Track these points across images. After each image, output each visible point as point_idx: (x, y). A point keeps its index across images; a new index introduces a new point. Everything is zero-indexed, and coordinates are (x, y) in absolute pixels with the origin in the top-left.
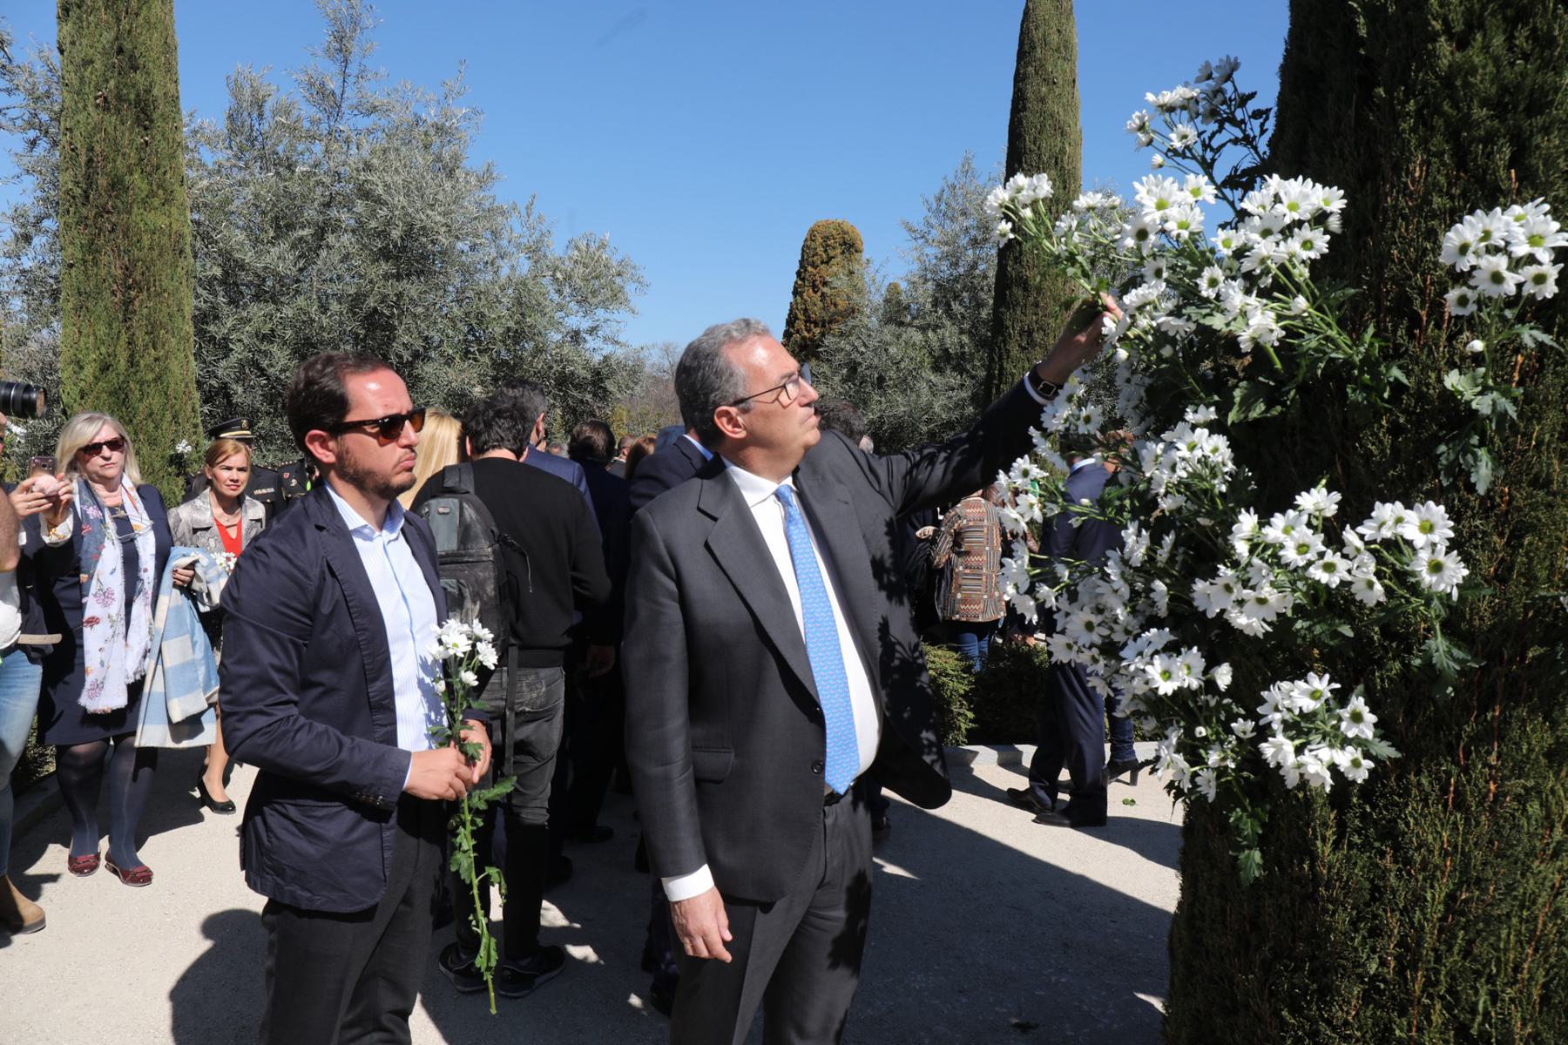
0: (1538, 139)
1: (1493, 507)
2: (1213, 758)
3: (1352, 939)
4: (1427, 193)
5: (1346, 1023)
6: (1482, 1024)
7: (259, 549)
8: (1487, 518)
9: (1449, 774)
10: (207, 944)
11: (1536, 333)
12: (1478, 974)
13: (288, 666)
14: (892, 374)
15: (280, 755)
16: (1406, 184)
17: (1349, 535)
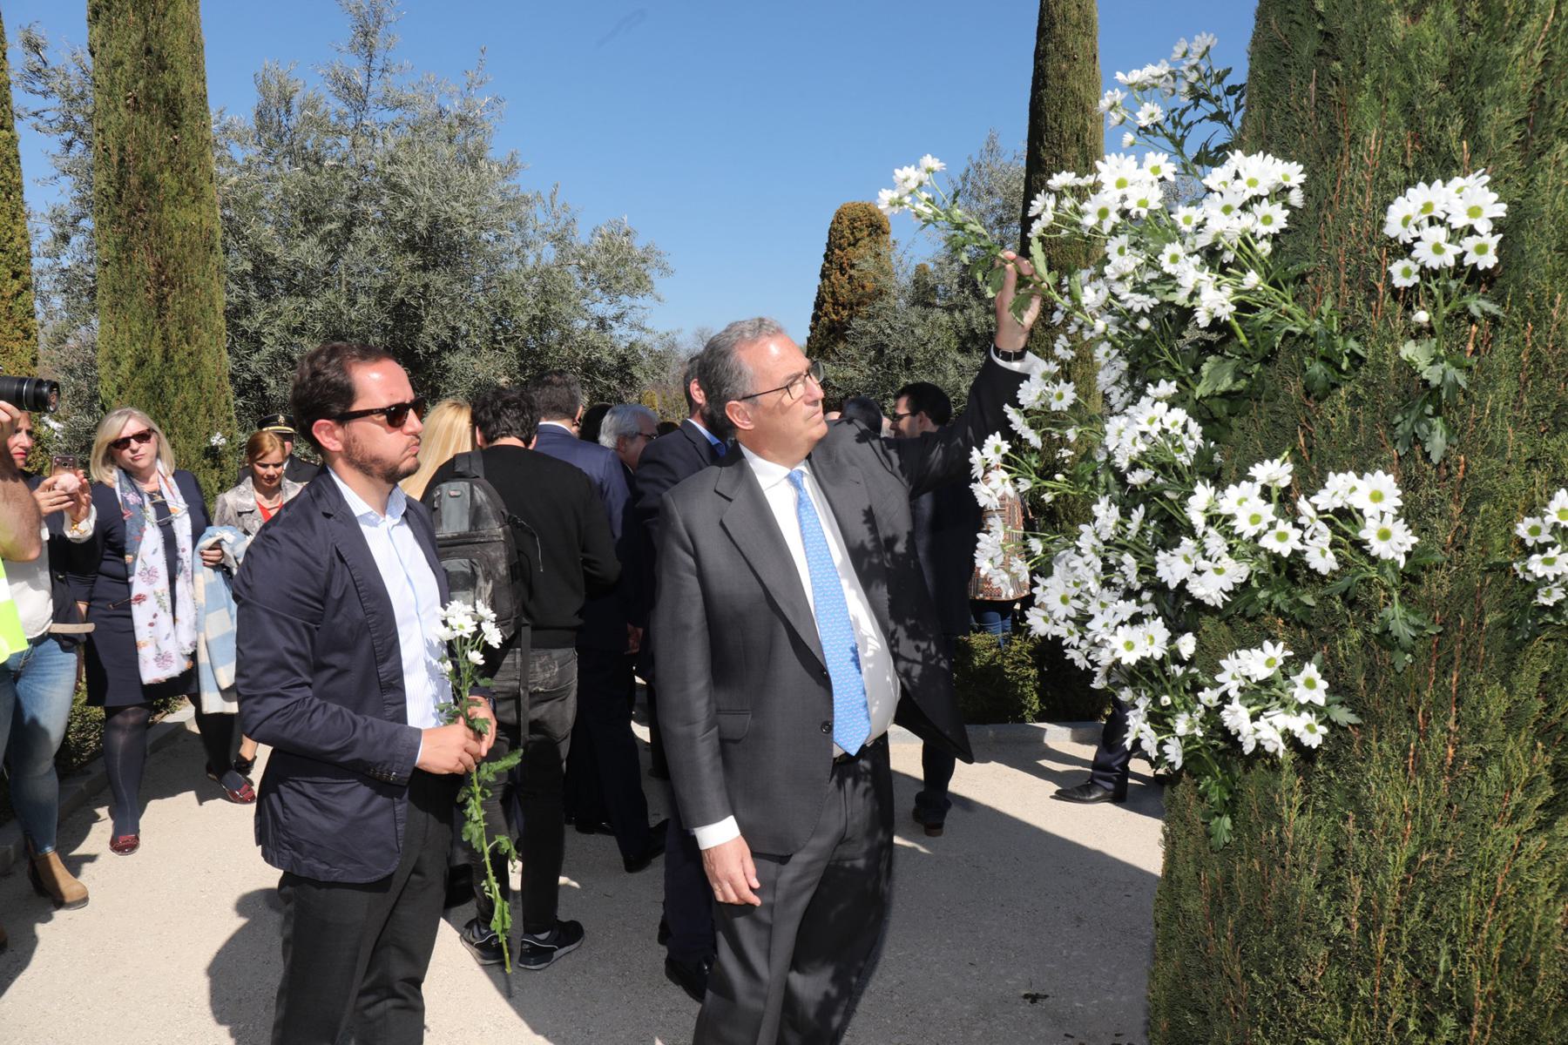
0: (1489, 110)
2: (1182, 725)
3: (1317, 902)
5: (1313, 984)
7: (270, 537)
10: (241, 922)
11: (1483, 303)
13: (302, 650)
14: (919, 355)
15: (297, 735)
17: (1302, 504)
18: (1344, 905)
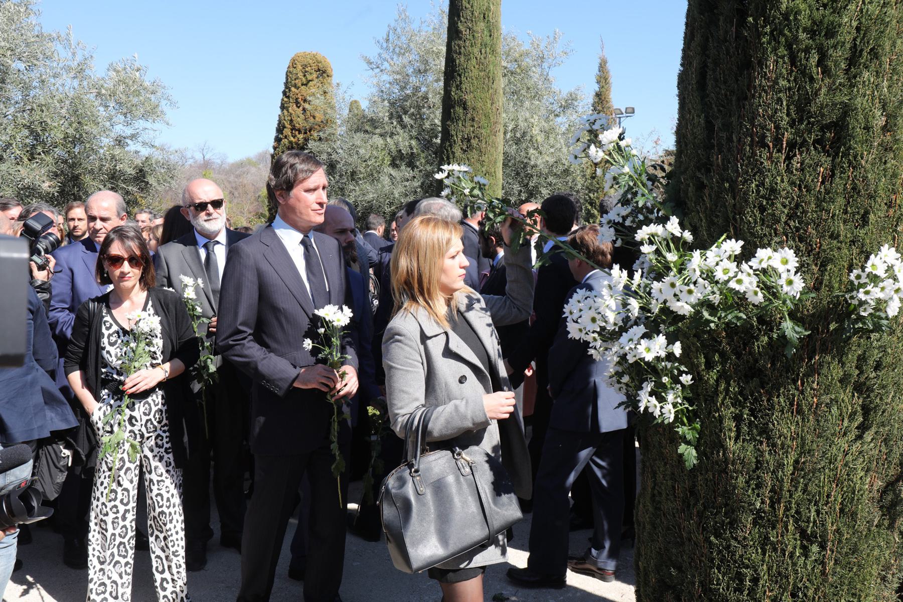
0: (831, 51)
1: (812, 250)
2: (670, 397)
3: (747, 491)
4: (777, 78)
5: (745, 538)
6: (813, 527)
8: (809, 256)
9: (793, 395)
12: (810, 501)
16: (765, 73)
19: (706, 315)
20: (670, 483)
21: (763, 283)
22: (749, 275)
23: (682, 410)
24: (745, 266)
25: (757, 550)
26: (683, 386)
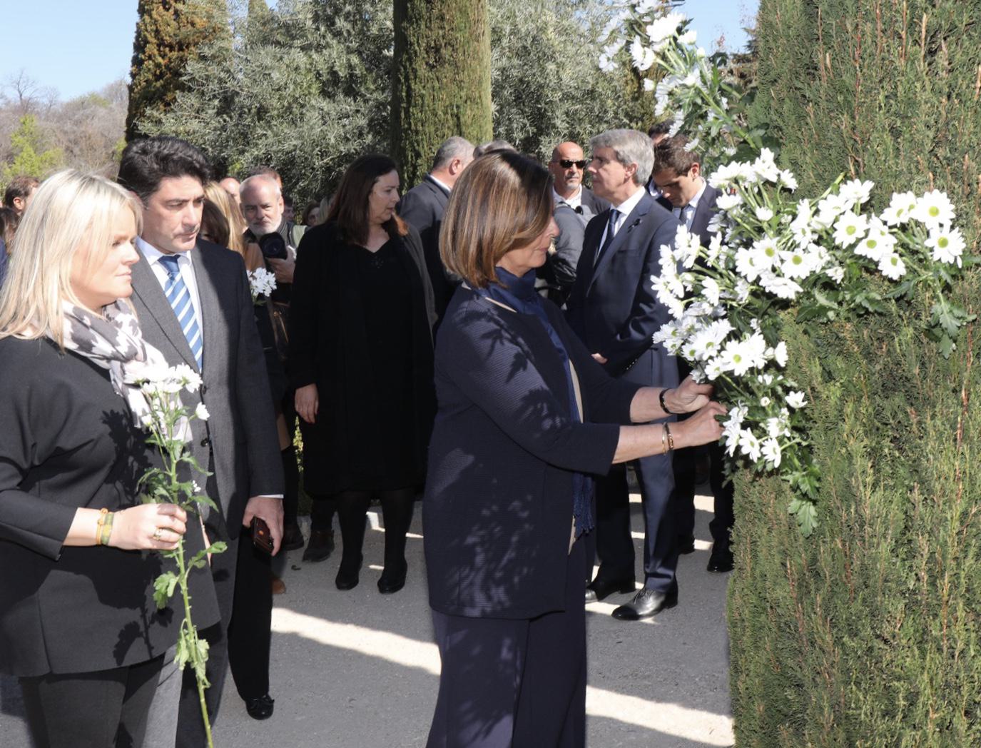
3: (894, 564)
9: (956, 413)
14: (275, 102)
18: (917, 561)
19: (821, 298)
20: (777, 559)
21: (904, 245)
22: (882, 233)
23: (791, 447)
24: (875, 222)
25: (913, 651)
26: (791, 410)
